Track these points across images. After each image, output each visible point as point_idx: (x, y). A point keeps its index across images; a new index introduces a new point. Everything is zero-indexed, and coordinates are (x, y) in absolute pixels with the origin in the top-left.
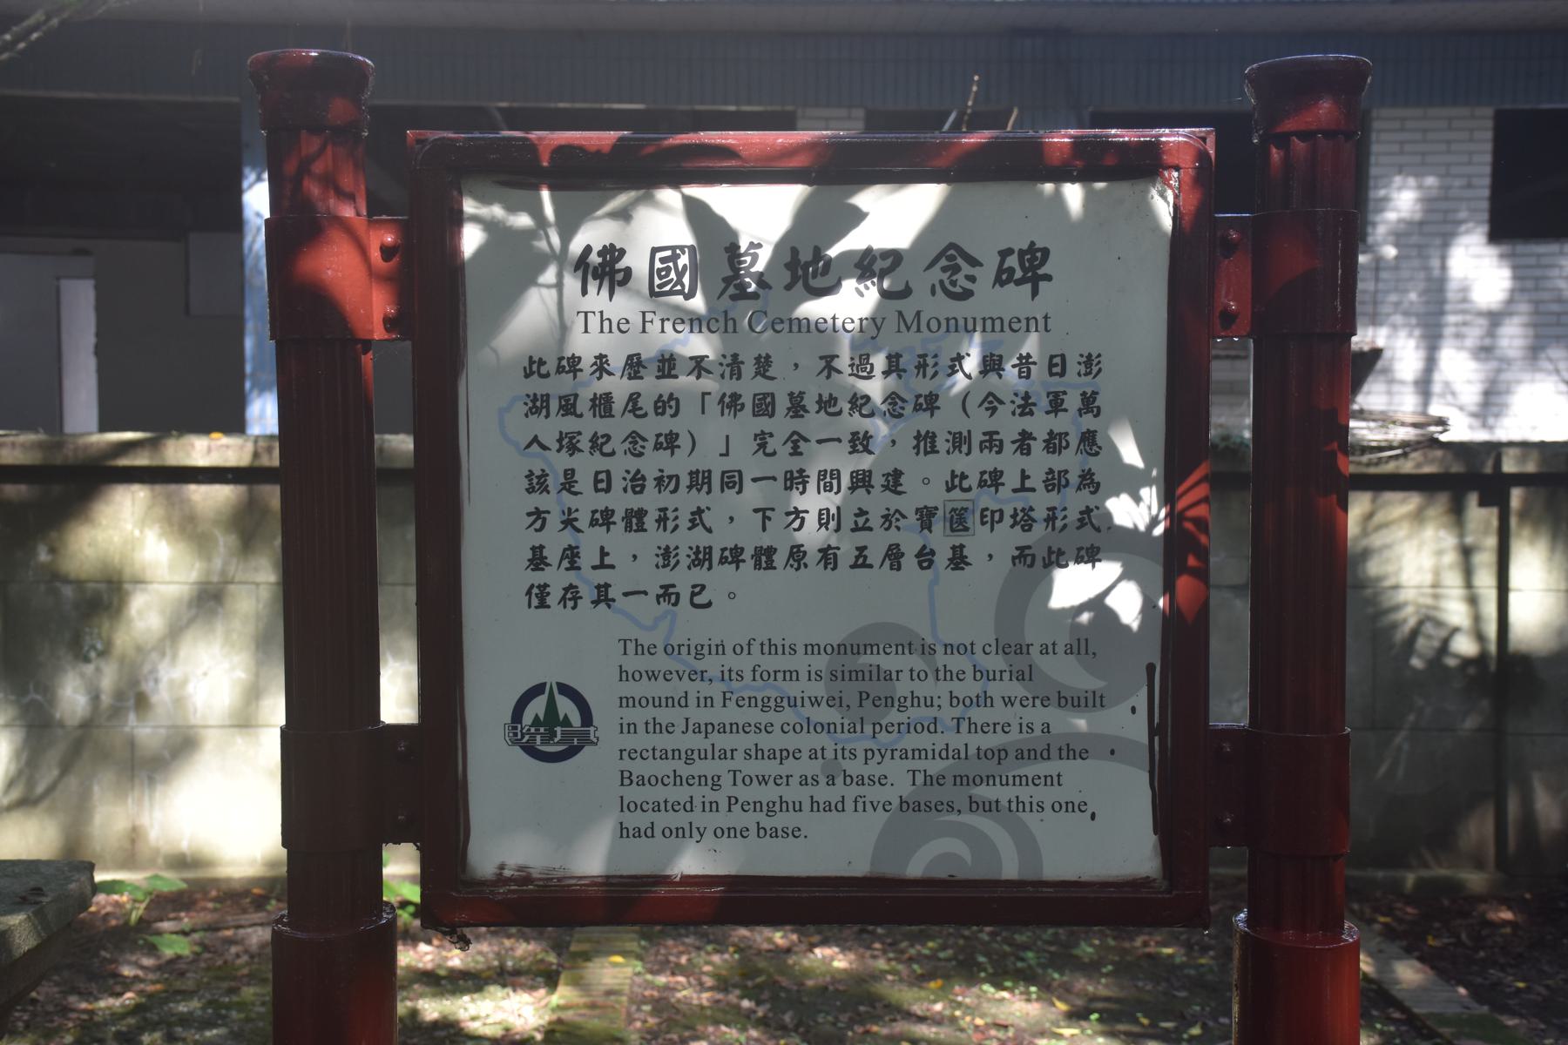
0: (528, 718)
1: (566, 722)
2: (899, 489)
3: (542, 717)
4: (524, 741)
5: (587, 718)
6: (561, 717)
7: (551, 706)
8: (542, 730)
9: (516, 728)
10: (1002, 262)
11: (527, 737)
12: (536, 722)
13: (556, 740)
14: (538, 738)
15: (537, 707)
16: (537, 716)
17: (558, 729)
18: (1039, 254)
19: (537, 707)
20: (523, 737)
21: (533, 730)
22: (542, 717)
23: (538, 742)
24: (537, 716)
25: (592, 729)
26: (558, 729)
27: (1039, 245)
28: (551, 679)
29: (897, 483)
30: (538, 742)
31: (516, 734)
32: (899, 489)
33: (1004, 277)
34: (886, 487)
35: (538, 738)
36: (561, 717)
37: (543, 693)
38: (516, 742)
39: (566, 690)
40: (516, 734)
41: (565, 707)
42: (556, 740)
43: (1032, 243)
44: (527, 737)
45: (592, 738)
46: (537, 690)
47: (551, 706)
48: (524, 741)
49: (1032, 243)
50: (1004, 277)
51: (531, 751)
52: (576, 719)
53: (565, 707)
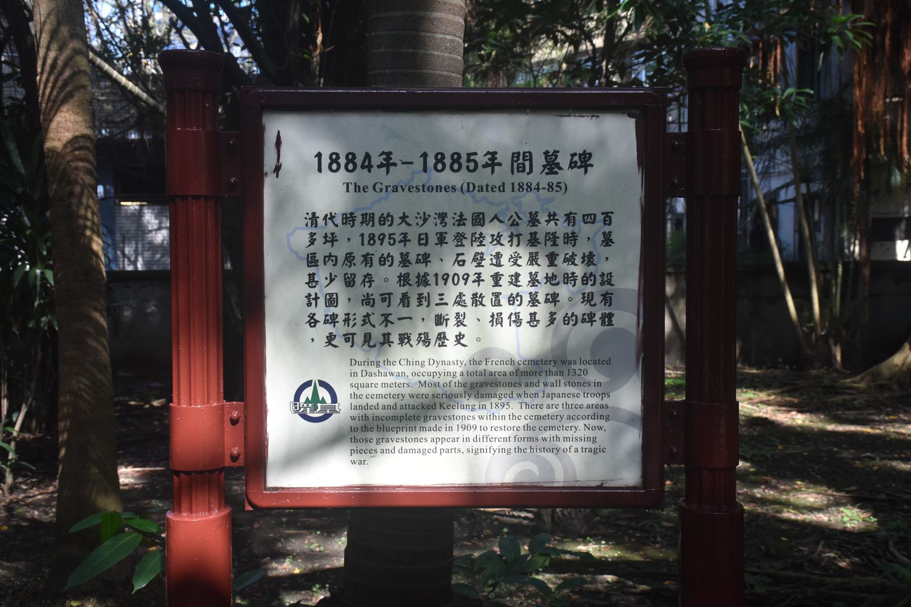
0: (303, 399)
1: (323, 401)
2: (518, 284)
3: (310, 399)
4: (301, 411)
5: (334, 399)
6: (320, 399)
7: (315, 392)
8: (310, 405)
9: (296, 404)
10: (572, 159)
11: (302, 409)
12: (307, 401)
13: (318, 411)
14: (308, 409)
15: (307, 393)
16: (307, 398)
17: (319, 405)
18: (587, 156)
19: (307, 393)
20: (300, 409)
21: (305, 405)
22: (310, 399)
23: (308, 411)
24: (307, 398)
25: (337, 405)
26: (319, 405)
27: (588, 151)
28: (315, 378)
29: (517, 281)
30: (308, 411)
31: (296, 408)
32: (518, 284)
33: (573, 165)
34: (511, 283)
35: (308, 409)
36: (320, 399)
37: (311, 385)
38: (295, 412)
39: (323, 384)
40: (296, 408)
41: (323, 393)
42: (318, 411)
43: (585, 151)
44: (302, 409)
45: (337, 409)
46: (308, 384)
47: (315, 392)
48: (301, 411)
49: (585, 151)
50: (573, 165)
51: (304, 416)
52: (328, 399)
53: (323, 393)
